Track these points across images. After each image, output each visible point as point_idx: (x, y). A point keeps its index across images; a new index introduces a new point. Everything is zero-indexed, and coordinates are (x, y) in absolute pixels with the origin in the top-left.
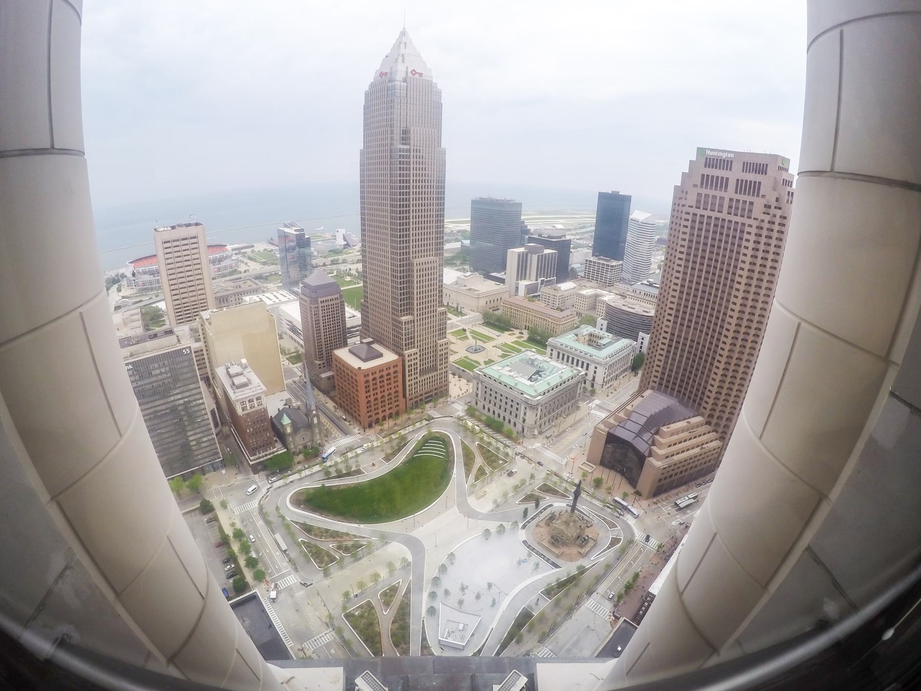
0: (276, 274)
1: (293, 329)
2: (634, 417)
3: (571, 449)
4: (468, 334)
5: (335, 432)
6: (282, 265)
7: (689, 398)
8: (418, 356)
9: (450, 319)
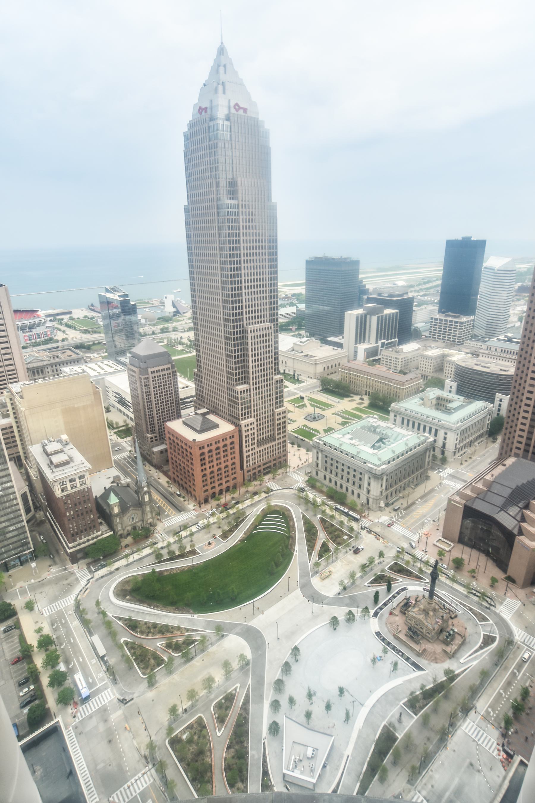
0: (99, 343)
1: (122, 401)
2: (496, 489)
3: (423, 524)
4: (306, 401)
5: (168, 509)
6: (106, 333)
8: (255, 426)
9: (287, 387)
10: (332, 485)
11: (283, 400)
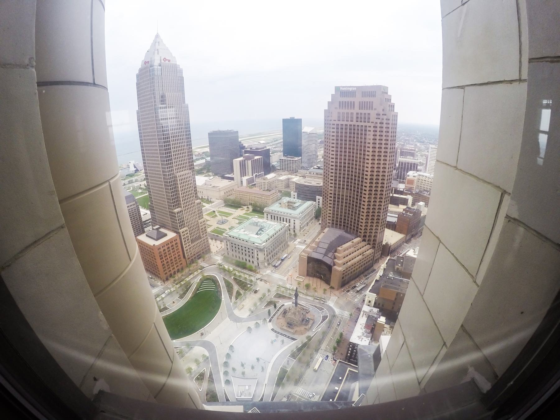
2: (321, 245)
3: (288, 271)
4: (216, 213)
7: (351, 228)
8: (188, 231)
10: (238, 259)
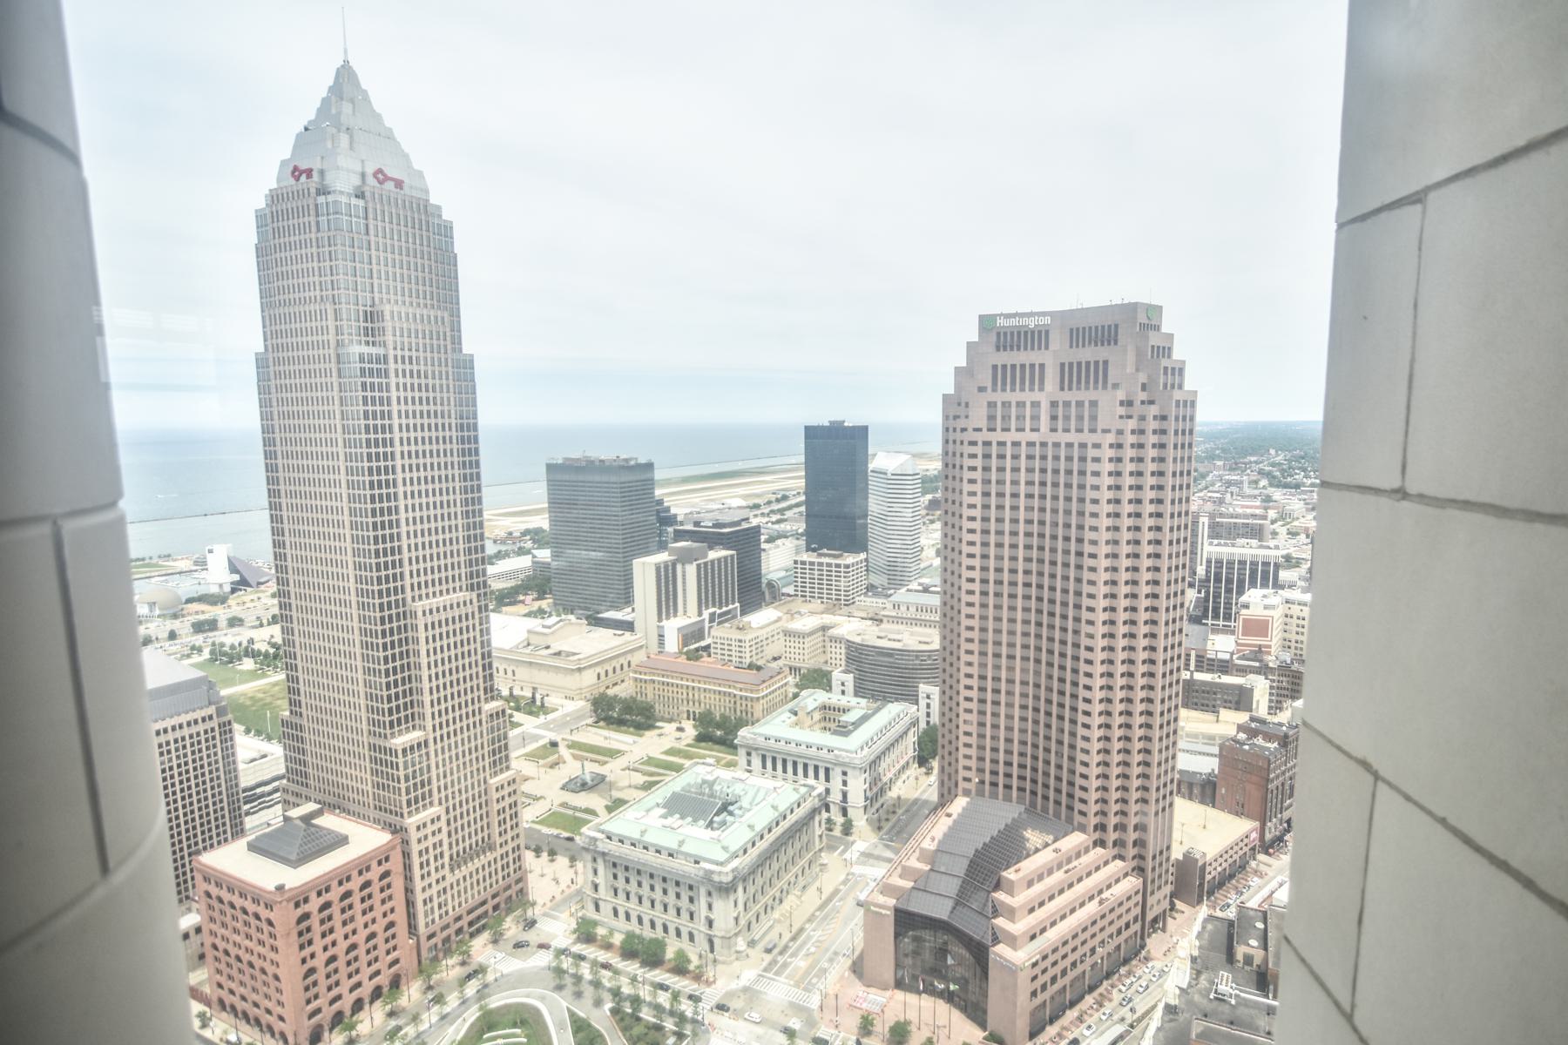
7: (1046, 798)
10: (633, 926)
11: (507, 757)
